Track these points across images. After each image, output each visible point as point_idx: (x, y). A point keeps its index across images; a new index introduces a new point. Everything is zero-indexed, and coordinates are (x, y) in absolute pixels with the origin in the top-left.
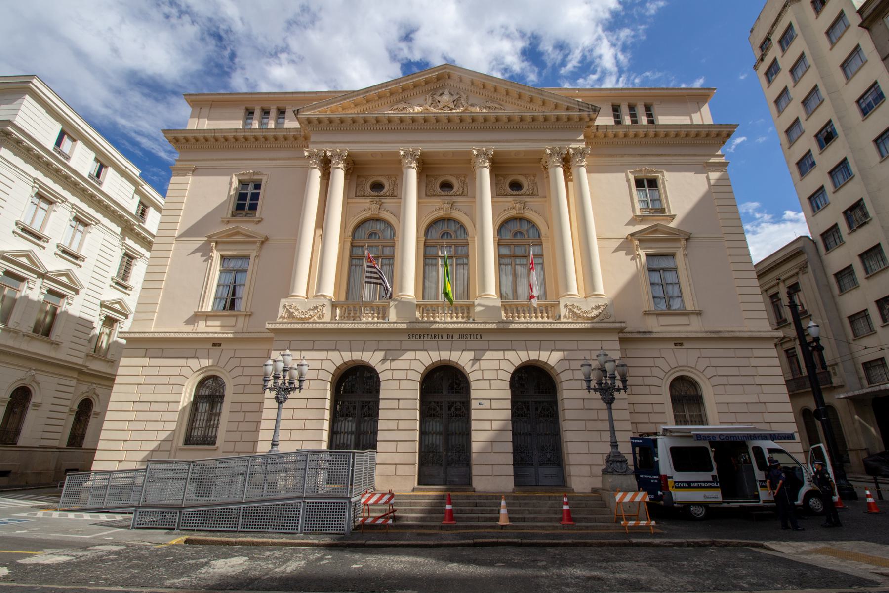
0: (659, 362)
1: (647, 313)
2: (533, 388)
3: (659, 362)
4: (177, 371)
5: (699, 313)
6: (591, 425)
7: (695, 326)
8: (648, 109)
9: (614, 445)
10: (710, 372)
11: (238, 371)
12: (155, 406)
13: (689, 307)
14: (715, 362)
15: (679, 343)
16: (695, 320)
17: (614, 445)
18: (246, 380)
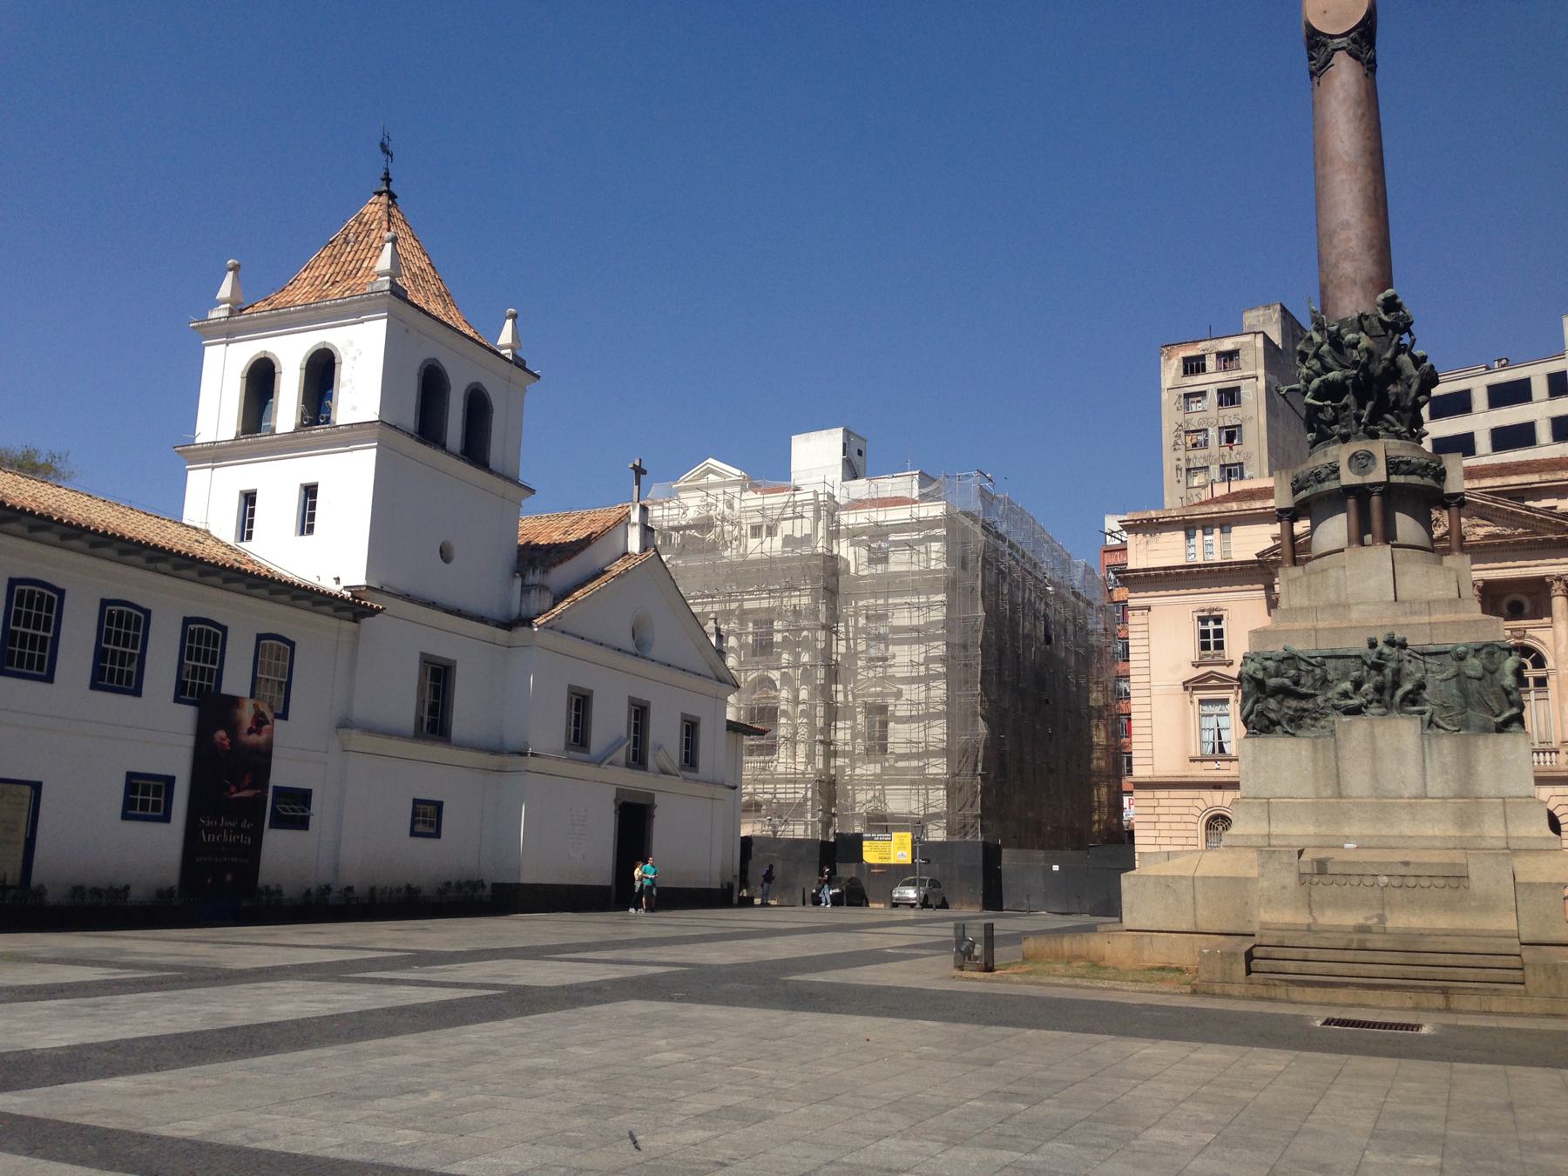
4: (1185, 810)
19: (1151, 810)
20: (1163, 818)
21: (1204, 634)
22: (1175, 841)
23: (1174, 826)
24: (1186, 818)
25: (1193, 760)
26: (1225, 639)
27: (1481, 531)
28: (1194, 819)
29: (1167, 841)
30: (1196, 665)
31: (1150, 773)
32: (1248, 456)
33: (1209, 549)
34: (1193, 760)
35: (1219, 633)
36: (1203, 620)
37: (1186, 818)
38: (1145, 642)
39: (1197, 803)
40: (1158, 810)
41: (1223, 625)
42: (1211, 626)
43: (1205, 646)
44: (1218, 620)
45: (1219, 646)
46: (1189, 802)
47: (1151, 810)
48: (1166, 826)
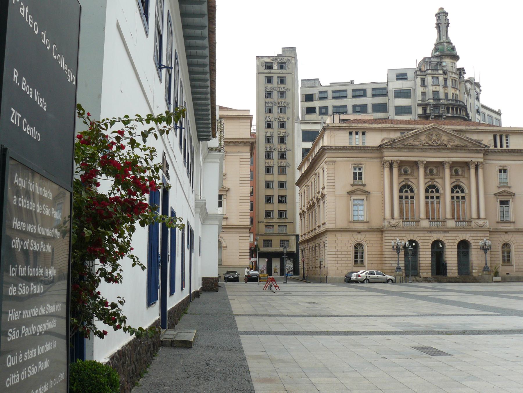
0: (500, 239)
1: (498, 222)
2: (464, 247)
3: (500, 239)
4: (347, 242)
5: (514, 223)
6: (479, 258)
7: (511, 227)
8: (507, 137)
9: (486, 264)
10: (515, 242)
11: (368, 242)
12: (343, 253)
13: (512, 220)
14: (516, 239)
15: (506, 232)
16: (512, 224)
17: (486, 264)
18: (371, 245)
19: (334, 242)
20: (339, 245)
21: (355, 174)
22: (343, 253)
23: (343, 247)
24: (347, 245)
25: (350, 222)
26: (363, 176)
27: (452, 144)
28: (350, 245)
29: (340, 253)
30: (352, 185)
31: (334, 227)
32: (288, 104)
33: (357, 141)
34: (350, 222)
35: (360, 174)
36: (355, 169)
37: (347, 245)
38: (333, 175)
39: (352, 239)
40: (337, 242)
41: (362, 171)
42: (357, 171)
43: (355, 179)
44: (360, 169)
45: (360, 179)
46: (349, 238)
47: (334, 242)
48: (340, 248)
